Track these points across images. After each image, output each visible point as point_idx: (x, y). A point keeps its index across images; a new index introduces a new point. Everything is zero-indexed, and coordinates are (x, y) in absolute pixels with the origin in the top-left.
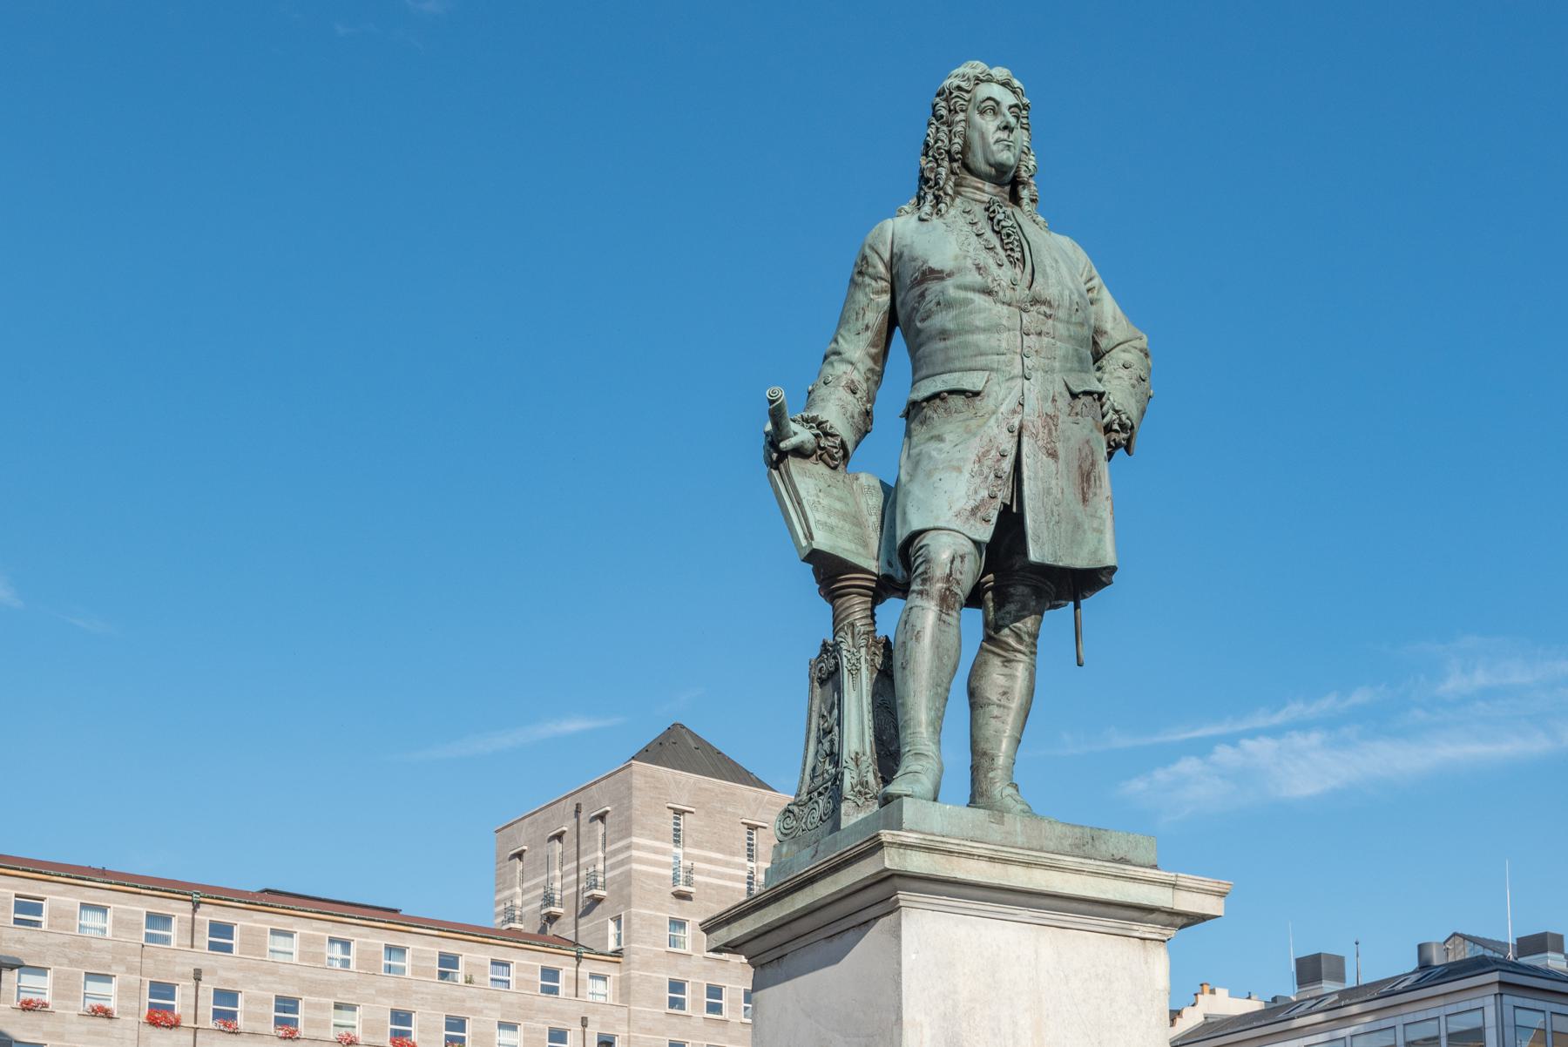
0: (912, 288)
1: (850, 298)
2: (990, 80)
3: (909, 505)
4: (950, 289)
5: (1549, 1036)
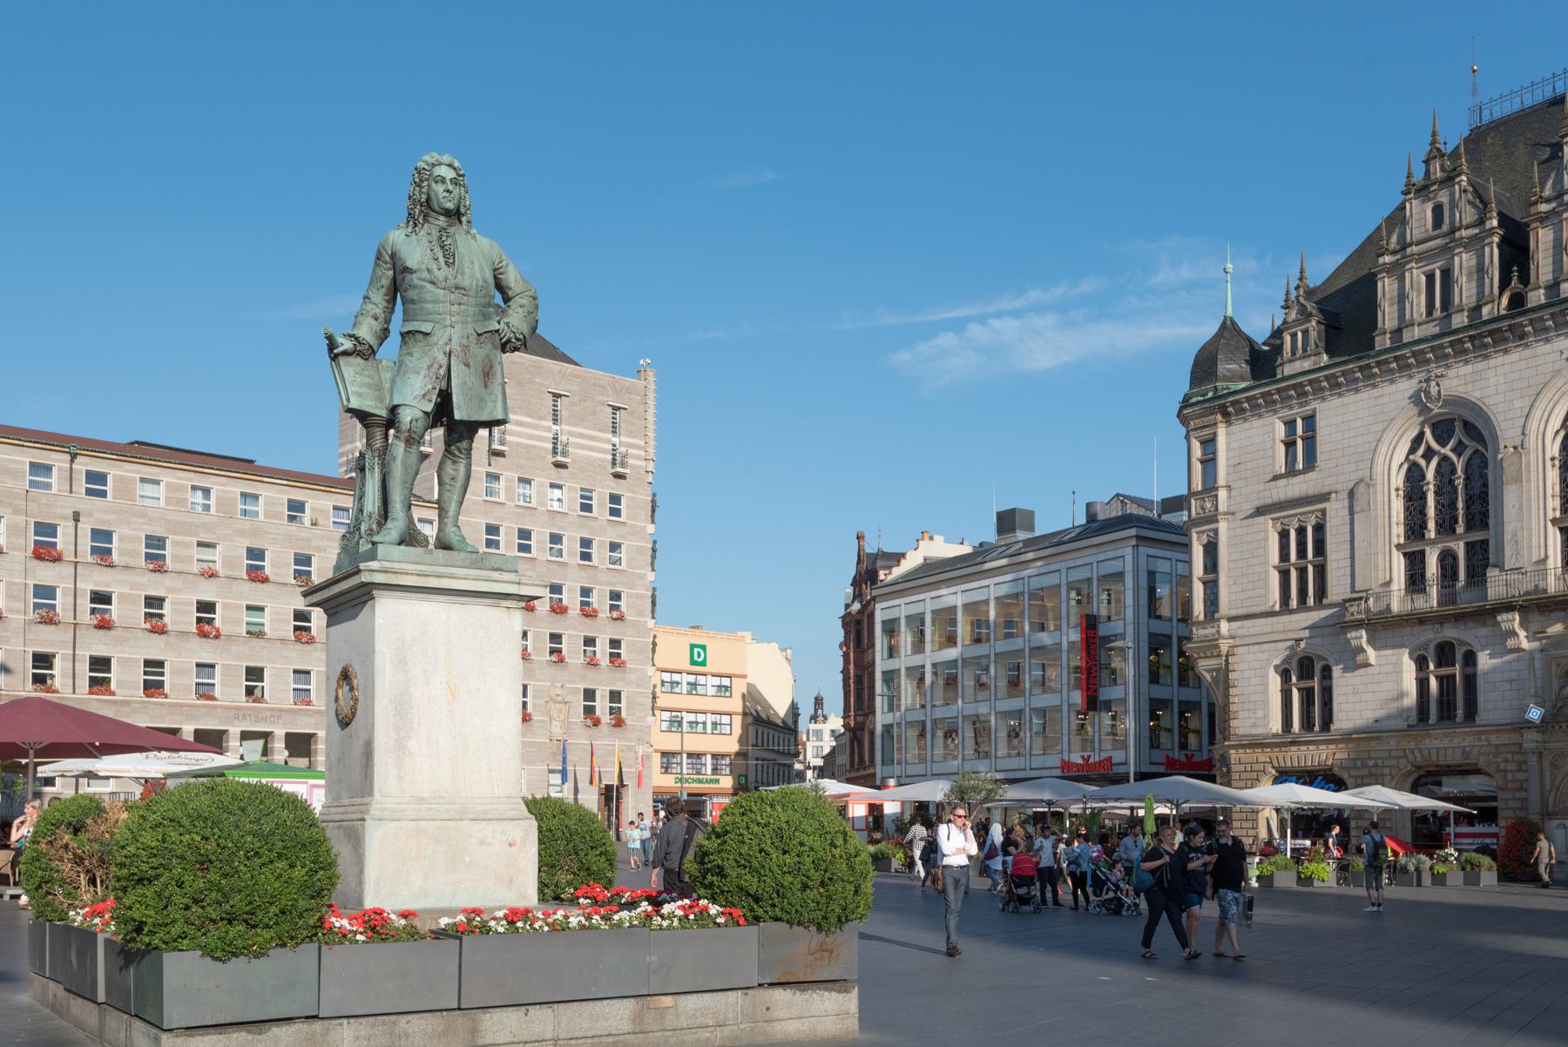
1: (374, 271)
2: (441, 164)
4: (414, 279)
5: (1174, 579)
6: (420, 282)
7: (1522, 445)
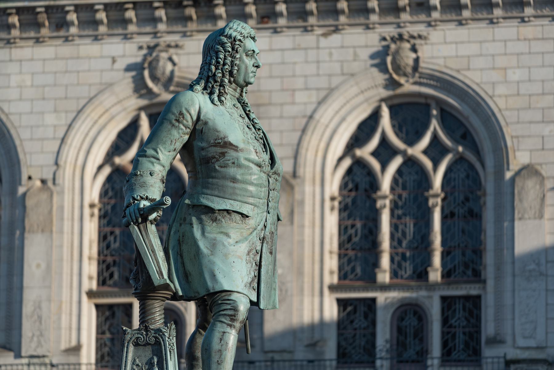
3: (217, 273)
6: (246, 163)
7: (54, 179)
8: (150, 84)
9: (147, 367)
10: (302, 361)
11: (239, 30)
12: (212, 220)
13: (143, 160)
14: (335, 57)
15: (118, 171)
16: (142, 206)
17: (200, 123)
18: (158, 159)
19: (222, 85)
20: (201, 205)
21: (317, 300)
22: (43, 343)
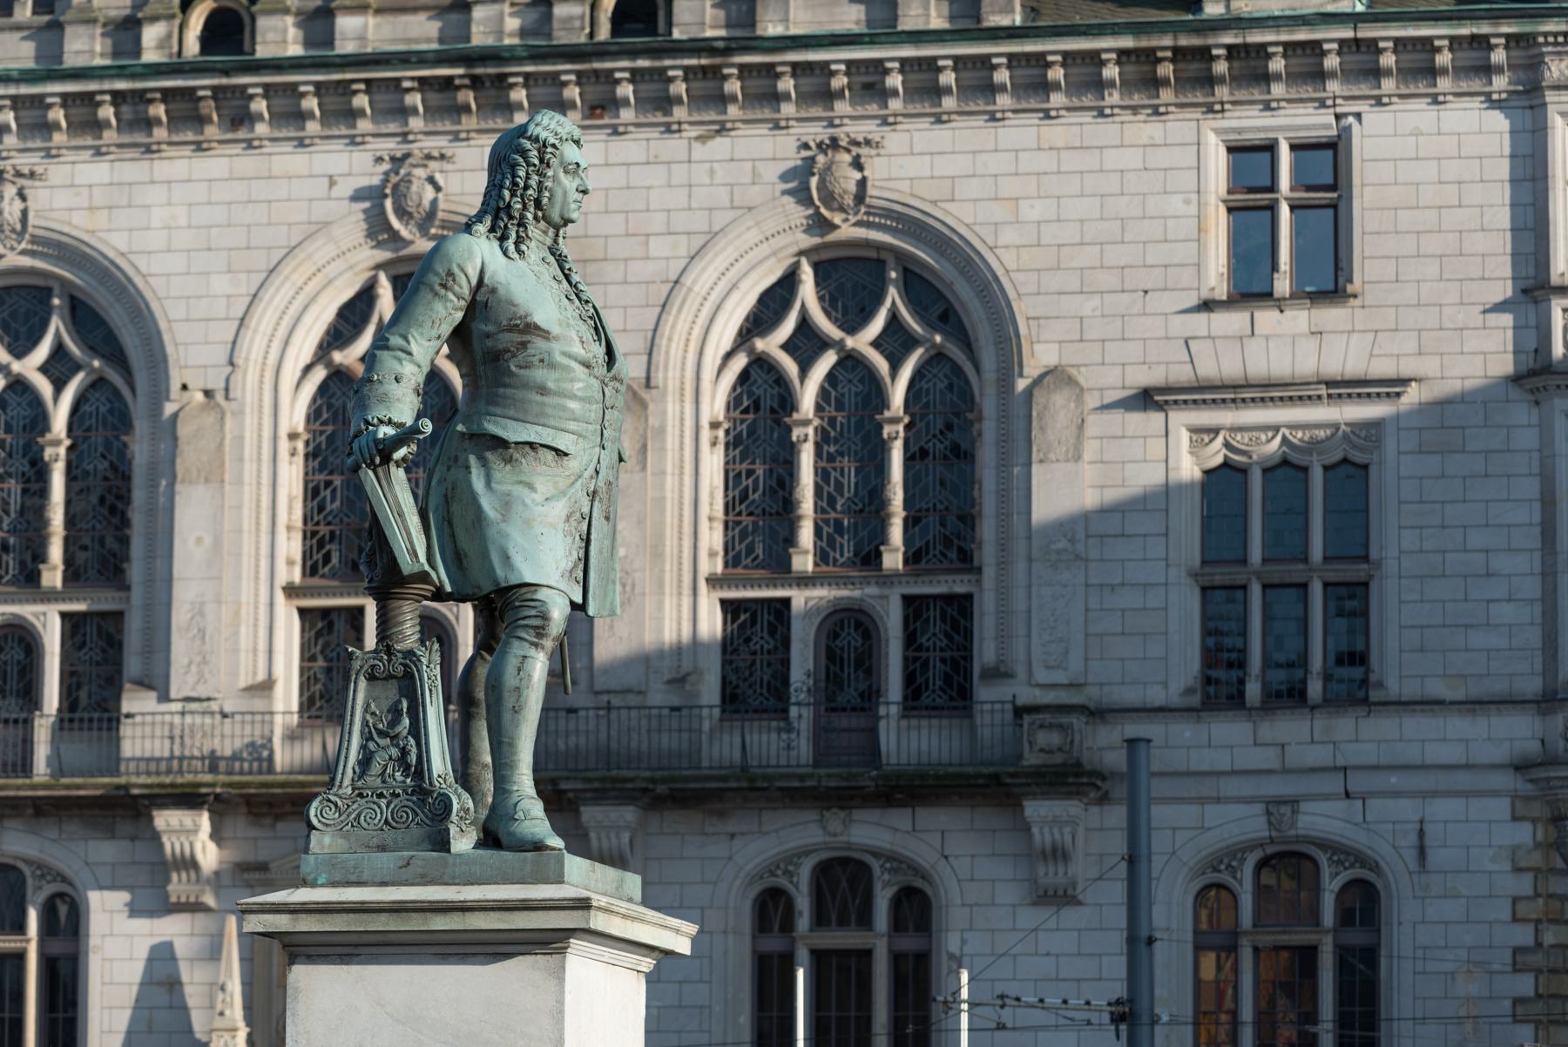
0: (510, 331)
3: (512, 552)
7: (227, 390)
8: (396, 223)
9: (390, 717)
10: (660, 708)
11: (552, 127)
12: (504, 460)
13: (384, 355)
14: (719, 179)
15: (338, 376)
16: (381, 435)
17: (483, 290)
18: (410, 354)
19: (522, 224)
20: (484, 435)
21: (686, 602)
22: (207, 675)
